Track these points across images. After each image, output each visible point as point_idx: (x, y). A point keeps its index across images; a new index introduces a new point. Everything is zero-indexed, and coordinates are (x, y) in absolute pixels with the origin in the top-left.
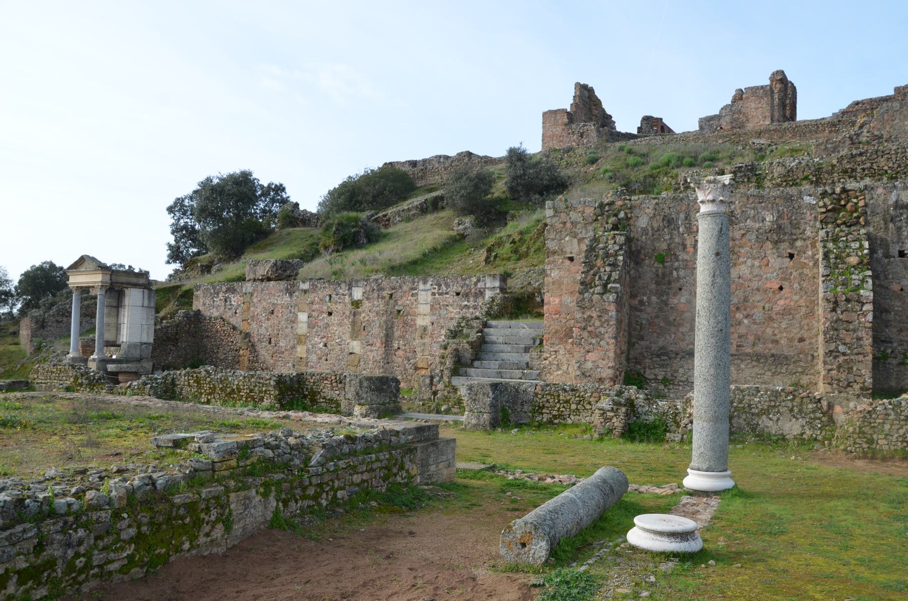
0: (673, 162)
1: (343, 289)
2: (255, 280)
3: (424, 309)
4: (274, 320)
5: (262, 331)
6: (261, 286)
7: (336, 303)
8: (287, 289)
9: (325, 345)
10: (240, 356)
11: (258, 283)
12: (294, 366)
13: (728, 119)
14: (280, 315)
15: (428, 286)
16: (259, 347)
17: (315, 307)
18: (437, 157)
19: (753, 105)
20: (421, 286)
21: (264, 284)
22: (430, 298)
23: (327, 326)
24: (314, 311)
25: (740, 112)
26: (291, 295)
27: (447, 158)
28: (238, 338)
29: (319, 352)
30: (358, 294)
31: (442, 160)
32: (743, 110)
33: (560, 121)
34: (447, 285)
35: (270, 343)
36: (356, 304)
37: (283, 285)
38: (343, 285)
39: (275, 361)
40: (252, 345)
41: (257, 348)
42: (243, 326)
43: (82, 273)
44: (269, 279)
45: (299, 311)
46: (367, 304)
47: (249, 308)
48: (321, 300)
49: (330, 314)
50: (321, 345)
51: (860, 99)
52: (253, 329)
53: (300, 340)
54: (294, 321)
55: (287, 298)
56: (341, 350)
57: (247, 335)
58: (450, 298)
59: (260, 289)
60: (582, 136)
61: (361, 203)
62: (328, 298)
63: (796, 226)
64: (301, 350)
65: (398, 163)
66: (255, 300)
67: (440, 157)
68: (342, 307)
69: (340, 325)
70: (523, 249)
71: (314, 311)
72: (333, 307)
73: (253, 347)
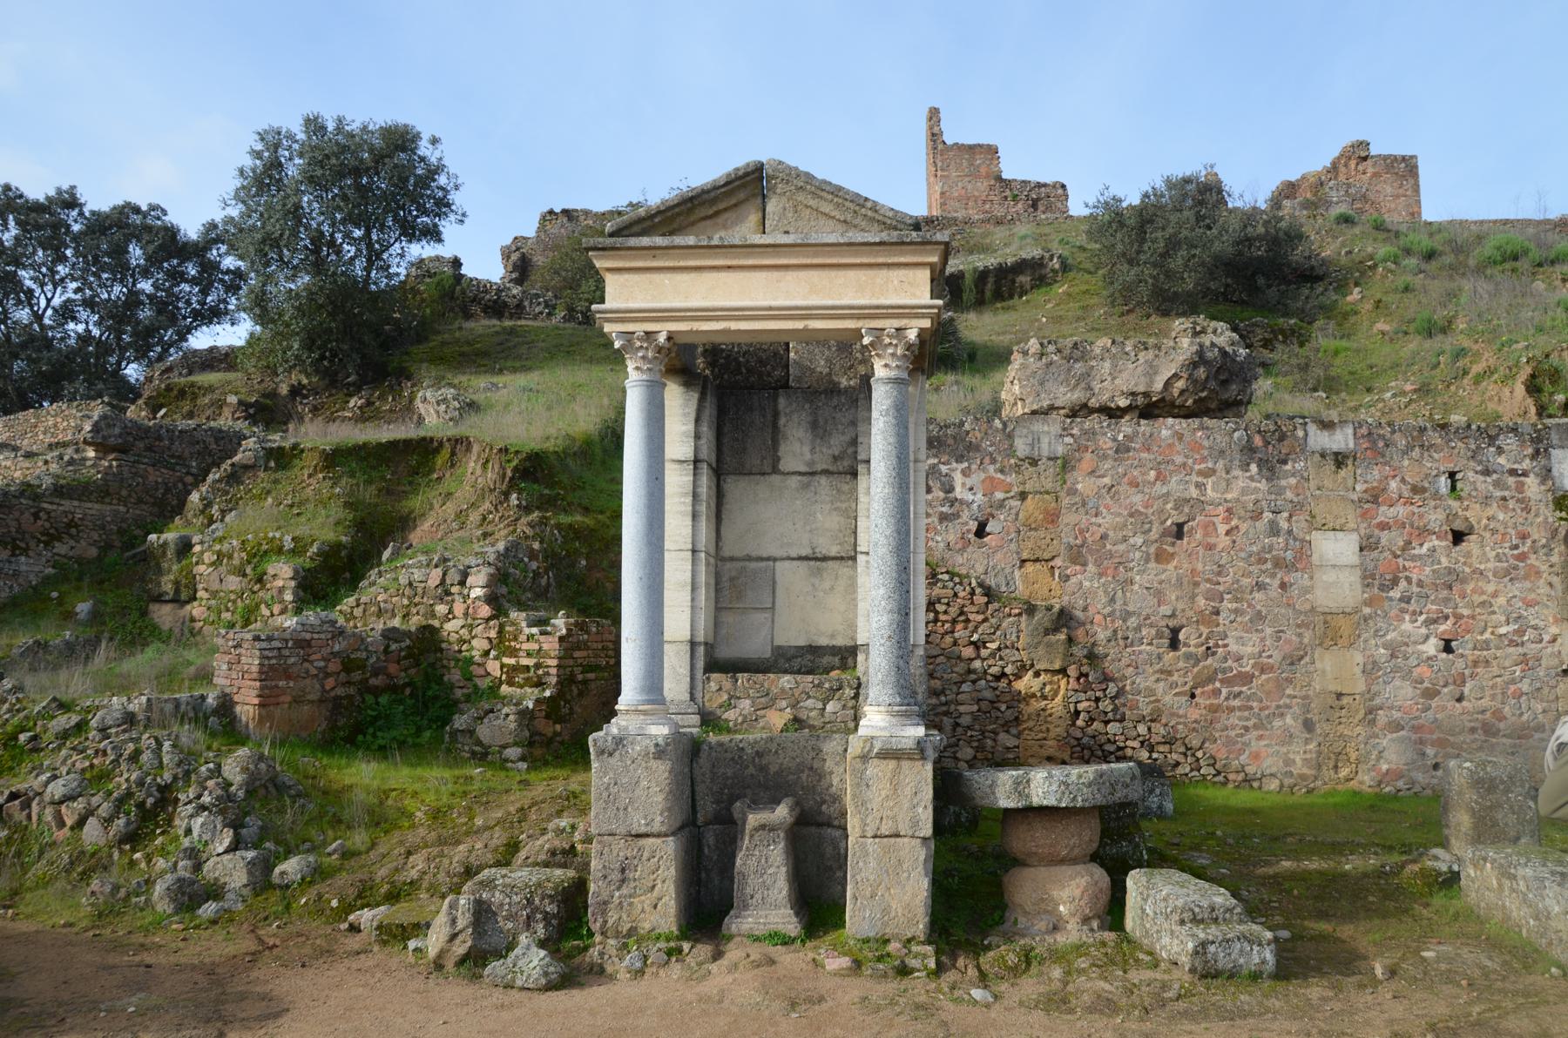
0: (1535, 254)
1: (1511, 454)
2: (1079, 411)
4: (1187, 558)
5: (1138, 599)
6: (1109, 434)
7: (1486, 500)
8: (1249, 450)
9: (1448, 648)
10: (1019, 698)
11: (1093, 422)
12: (1308, 726)
14: (1223, 541)
16: (1117, 661)
17: (1385, 513)
19: (1389, 190)
21: (1126, 426)
23: (1451, 580)
24: (1384, 526)
25: (1364, 198)
26: (1270, 469)
28: (1020, 632)
29: (1423, 670)
32: (1371, 195)
33: (983, 170)
35: (1174, 644)
37: (1221, 431)
38: (1509, 442)
39: (1214, 709)
40: (1092, 657)
41: (1110, 667)
42: (1022, 583)
44: (1150, 409)
45: (1315, 524)
47: (1053, 517)
48: (1416, 490)
49: (1458, 537)
50: (1432, 647)
52: (1085, 589)
53: (1330, 629)
54: (1300, 559)
55: (1246, 484)
56: (1524, 660)
57: (1064, 619)
59: (1106, 443)
60: (1034, 206)
62: (1443, 483)
64: (1335, 669)
65: (587, 213)
66: (1084, 485)
69: (1509, 574)
71: (1384, 526)
72: (1475, 514)
73: (1090, 667)
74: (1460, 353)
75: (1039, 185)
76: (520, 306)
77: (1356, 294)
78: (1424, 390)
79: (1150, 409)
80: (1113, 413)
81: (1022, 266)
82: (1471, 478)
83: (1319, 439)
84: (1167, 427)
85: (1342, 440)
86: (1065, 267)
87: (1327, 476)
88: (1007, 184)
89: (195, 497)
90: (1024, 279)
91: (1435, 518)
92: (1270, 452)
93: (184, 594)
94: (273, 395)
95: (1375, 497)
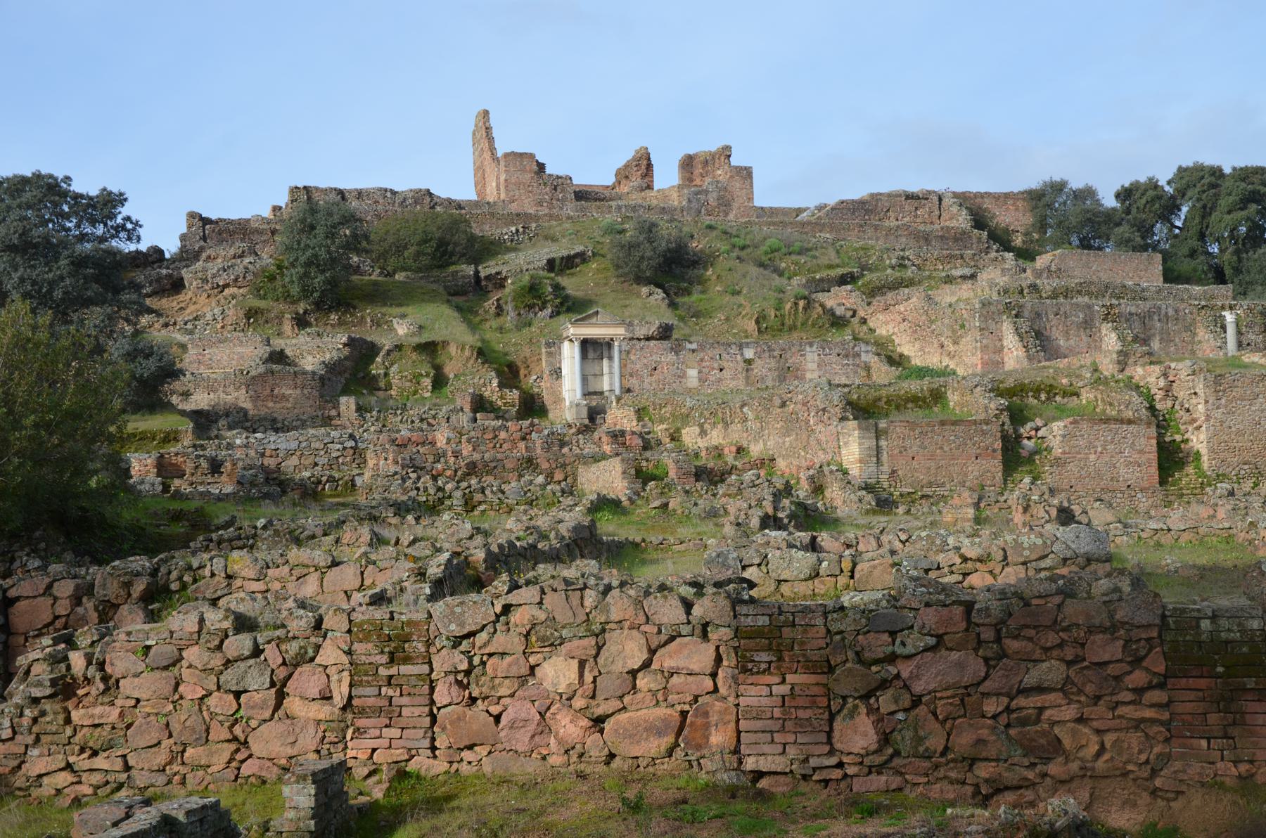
0: (784, 250)
1: (734, 349)
5: (646, 385)
13: (715, 195)
15: (814, 348)
17: (704, 364)
18: (380, 189)
20: (808, 349)
21: (642, 343)
22: (816, 358)
23: (719, 380)
26: (677, 353)
27: (394, 193)
30: (749, 353)
31: (389, 194)
34: (830, 349)
36: (749, 362)
44: (648, 339)
45: (688, 367)
46: (759, 362)
51: (845, 198)
55: (671, 357)
58: (833, 358)
60: (555, 189)
63: (1092, 320)
65: (317, 189)
67: (386, 190)
68: (733, 365)
70: (789, 322)
72: (725, 364)
74: (740, 306)
75: (558, 177)
76: (358, 267)
77: (710, 272)
78: (727, 319)
79: (648, 339)
80: (639, 339)
81: (577, 255)
82: (724, 355)
83: (689, 346)
84: (652, 343)
85: (694, 346)
86: (594, 254)
87: (691, 355)
89: (379, 359)
90: (578, 260)
91: (716, 365)
92: (676, 350)
93: (389, 387)
94: (297, 313)
95: (702, 360)
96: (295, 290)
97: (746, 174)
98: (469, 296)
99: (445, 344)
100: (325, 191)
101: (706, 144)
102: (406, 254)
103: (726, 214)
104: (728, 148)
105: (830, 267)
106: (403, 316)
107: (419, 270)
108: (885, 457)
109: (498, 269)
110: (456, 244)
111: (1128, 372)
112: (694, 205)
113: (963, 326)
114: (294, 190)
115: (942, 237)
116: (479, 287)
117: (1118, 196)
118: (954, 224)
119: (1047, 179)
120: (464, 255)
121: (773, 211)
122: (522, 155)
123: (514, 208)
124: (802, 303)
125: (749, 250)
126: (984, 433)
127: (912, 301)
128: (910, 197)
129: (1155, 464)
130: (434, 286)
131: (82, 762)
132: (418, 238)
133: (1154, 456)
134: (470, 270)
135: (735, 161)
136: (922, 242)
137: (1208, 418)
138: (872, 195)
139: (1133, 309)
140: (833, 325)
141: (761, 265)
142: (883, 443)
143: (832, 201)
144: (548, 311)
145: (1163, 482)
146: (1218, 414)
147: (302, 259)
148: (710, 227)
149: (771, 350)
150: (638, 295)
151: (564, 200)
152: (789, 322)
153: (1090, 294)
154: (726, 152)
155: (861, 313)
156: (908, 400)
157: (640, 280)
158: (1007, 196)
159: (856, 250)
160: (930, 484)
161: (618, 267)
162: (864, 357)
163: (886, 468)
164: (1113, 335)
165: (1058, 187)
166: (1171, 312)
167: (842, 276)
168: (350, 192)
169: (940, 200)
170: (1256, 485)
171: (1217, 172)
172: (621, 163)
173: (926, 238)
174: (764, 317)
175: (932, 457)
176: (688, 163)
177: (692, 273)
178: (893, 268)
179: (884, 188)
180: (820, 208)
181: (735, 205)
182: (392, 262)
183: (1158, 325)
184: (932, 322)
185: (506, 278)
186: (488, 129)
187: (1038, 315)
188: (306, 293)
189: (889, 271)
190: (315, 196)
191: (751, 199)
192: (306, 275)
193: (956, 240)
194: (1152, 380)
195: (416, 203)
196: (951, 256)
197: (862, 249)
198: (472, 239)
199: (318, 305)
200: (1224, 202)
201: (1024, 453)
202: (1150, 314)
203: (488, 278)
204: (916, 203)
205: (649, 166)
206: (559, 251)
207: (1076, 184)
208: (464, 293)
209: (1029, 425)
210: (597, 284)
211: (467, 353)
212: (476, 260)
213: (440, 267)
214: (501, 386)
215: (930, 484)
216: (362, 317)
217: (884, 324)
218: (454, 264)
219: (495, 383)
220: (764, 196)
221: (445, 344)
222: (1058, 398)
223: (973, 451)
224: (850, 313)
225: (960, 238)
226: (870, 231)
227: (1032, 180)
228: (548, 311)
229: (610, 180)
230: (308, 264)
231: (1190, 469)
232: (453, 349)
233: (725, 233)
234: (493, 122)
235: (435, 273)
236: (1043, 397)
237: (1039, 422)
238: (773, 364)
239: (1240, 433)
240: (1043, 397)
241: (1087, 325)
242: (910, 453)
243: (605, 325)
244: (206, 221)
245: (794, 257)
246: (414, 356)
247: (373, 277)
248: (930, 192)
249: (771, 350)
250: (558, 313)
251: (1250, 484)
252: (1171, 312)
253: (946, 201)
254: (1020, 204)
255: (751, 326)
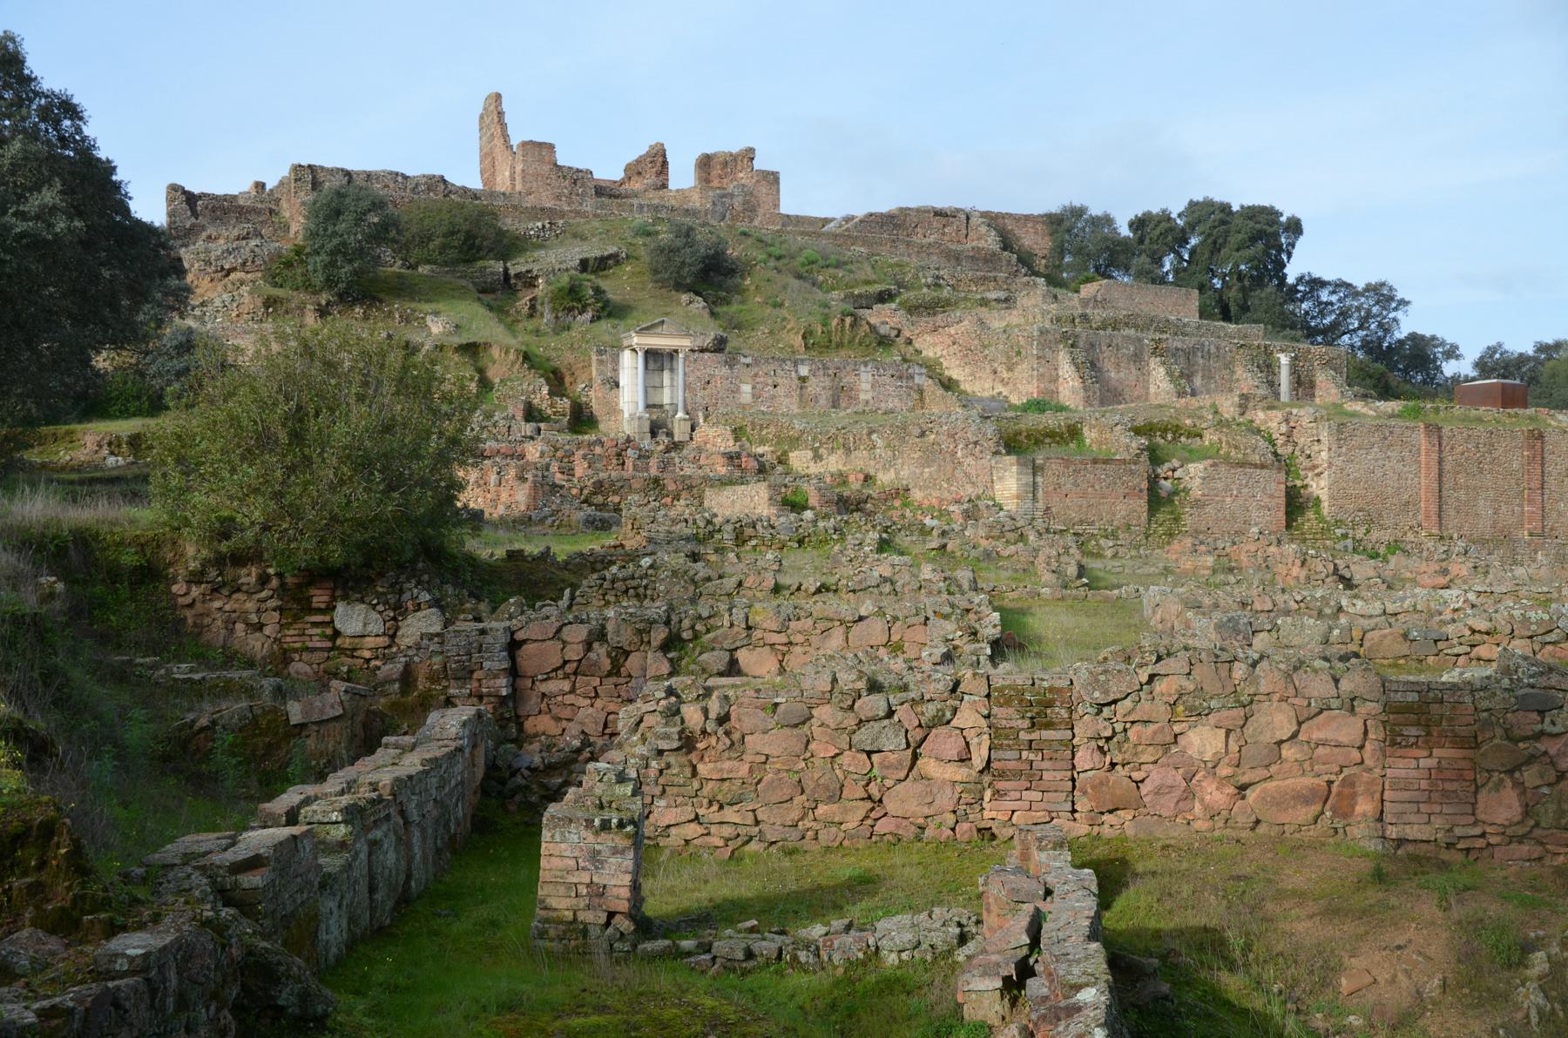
0: (821, 262)
1: (788, 366)
3: (865, 386)
4: (710, 390)
5: (698, 399)
13: (740, 199)
18: (391, 173)
23: (773, 397)
26: (731, 367)
27: (405, 177)
30: (804, 371)
36: (803, 379)
37: (720, 357)
43: (660, 335)
44: (702, 351)
46: (813, 379)
54: (737, 391)
55: (725, 370)
58: (887, 379)
61: (480, 249)
65: (322, 168)
68: (787, 382)
70: (836, 339)
72: (779, 381)
74: (784, 319)
75: (578, 171)
77: (748, 282)
78: (771, 333)
79: (702, 351)
81: (610, 257)
82: (779, 371)
83: (743, 360)
84: (706, 355)
85: (749, 360)
86: (628, 257)
87: (745, 369)
88: (560, 168)
92: (731, 363)
95: (756, 375)
96: (318, 279)
97: (772, 179)
98: (501, 292)
99: (487, 345)
100: (332, 172)
101: (727, 143)
102: (431, 246)
103: (751, 221)
104: (752, 150)
105: (867, 282)
106: (436, 313)
107: (446, 264)
108: (1040, 494)
109: (528, 267)
110: (485, 238)
111: (1248, 416)
112: (719, 208)
113: (1019, 353)
114: (297, 168)
115: (972, 257)
116: (508, 286)
117: (1131, 225)
118: (982, 244)
119: (1067, 204)
120: (491, 250)
121: (799, 220)
122: (540, 144)
123: (530, 201)
124: (848, 320)
125: (785, 261)
126: (1132, 473)
127: (962, 325)
128: (939, 213)
129: (1283, 509)
130: (463, 282)
131: (711, 814)
132: (444, 229)
133: (1282, 501)
134: (499, 267)
135: (758, 164)
136: (953, 262)
137: (1330, 465)
138: (901, 209)
139: (1179, 345)
140: (880, 344)
141: (799, 277)
142: (1039, 479)
143: (860, 212)
144: (588, 315)
145: (1288, 526)
146: (1339, 462)
147: (329, 247)
148: (744, 234)
149: (825, 368)
150: (679, 303)
151: (583, 195)
152: (836, 339)
153: (1136, 327)
154: (749, 154)
155: (906, 333)
156: (1047, 435)
157: (680, 286)
158: (1027, 218)
159: (891, 266)
160: (1081, 522)
161: (656, 272)
162: (917, 380)
163: (1041, 505)
164: (1162, 370)
165: (1078, 212)
166: (1213, 350)
167: (881, 293)
168: (358, 173)
169: (968, 219)
170: (1368, 531)
171: (1225, 208)
172: (632, 157)
173: (957, 258)
174: (811, 333)
175: (1084, 495)
176: (705, 164)
177: (729, 282)
178: (929, 287)
179: (913, 203)
180: (848, 219)
181: (761, 211)
182: (416, 253)
183: (1201, 361)
184: (985, 347)
185: (537, 277)
186: (501, 114)
187: (1092, 345)
188: (330, 283)
189: (925, 290)
190: (321, 176)
191: (777, 206)
192: (332, 264)
193: (986, 261)
194: (1274, 425)
195: (429, 189)
196: (985, 278)
197: (897, 265)
198: (501, 233)
199: (342, 297)
200: (1234, 239)
201: (1163, 494)
202: (1194, 350)
203: (518, 276)
204: (944, 220)
205: (665, 163)
206: (593, 251)
207: (1096, 210)
208: (493, 291)
209: (1167, 465)
210: (634, 289)
211: (512, 356)
212: (504, 256)
213: (467, 261)
214: (551, 393)
215: (1081, 522)
216: (390, 312)
217: (931, 346)
218: (481, 259)
219: (545, 390)
220: (792, 202)
221: (487, 345)
222: (1183, 439)
223: (1121, 490)
224: (894, 333)
225: (990, 259)
226: (902, 247)
227: (1049, 202)
228: (588, 315)
229: (617, 174)
230: (332, 253)
231: (1310, 515)
232: (495, 352)
233: (760, 241)
234: (505, 107)
235: (462, 268)
236: (1169, 436)
237: (1176, 463)
238: (827, 382)
239: (1357, 481)
240: (1169, 436)
241: (1137, 358)
242: (1064, 490)
243: (671, 335)
244: (191, 199)
245: (831, 270)
246: (456, 357)
247: (395, 269)
248: (958, 210)
249: (825, 368)
250: (599, 318)
251: (1363, 530)
252: (1213, 350)
253: (974, 221)
254: (1039, 227)
255: (798, 341)
